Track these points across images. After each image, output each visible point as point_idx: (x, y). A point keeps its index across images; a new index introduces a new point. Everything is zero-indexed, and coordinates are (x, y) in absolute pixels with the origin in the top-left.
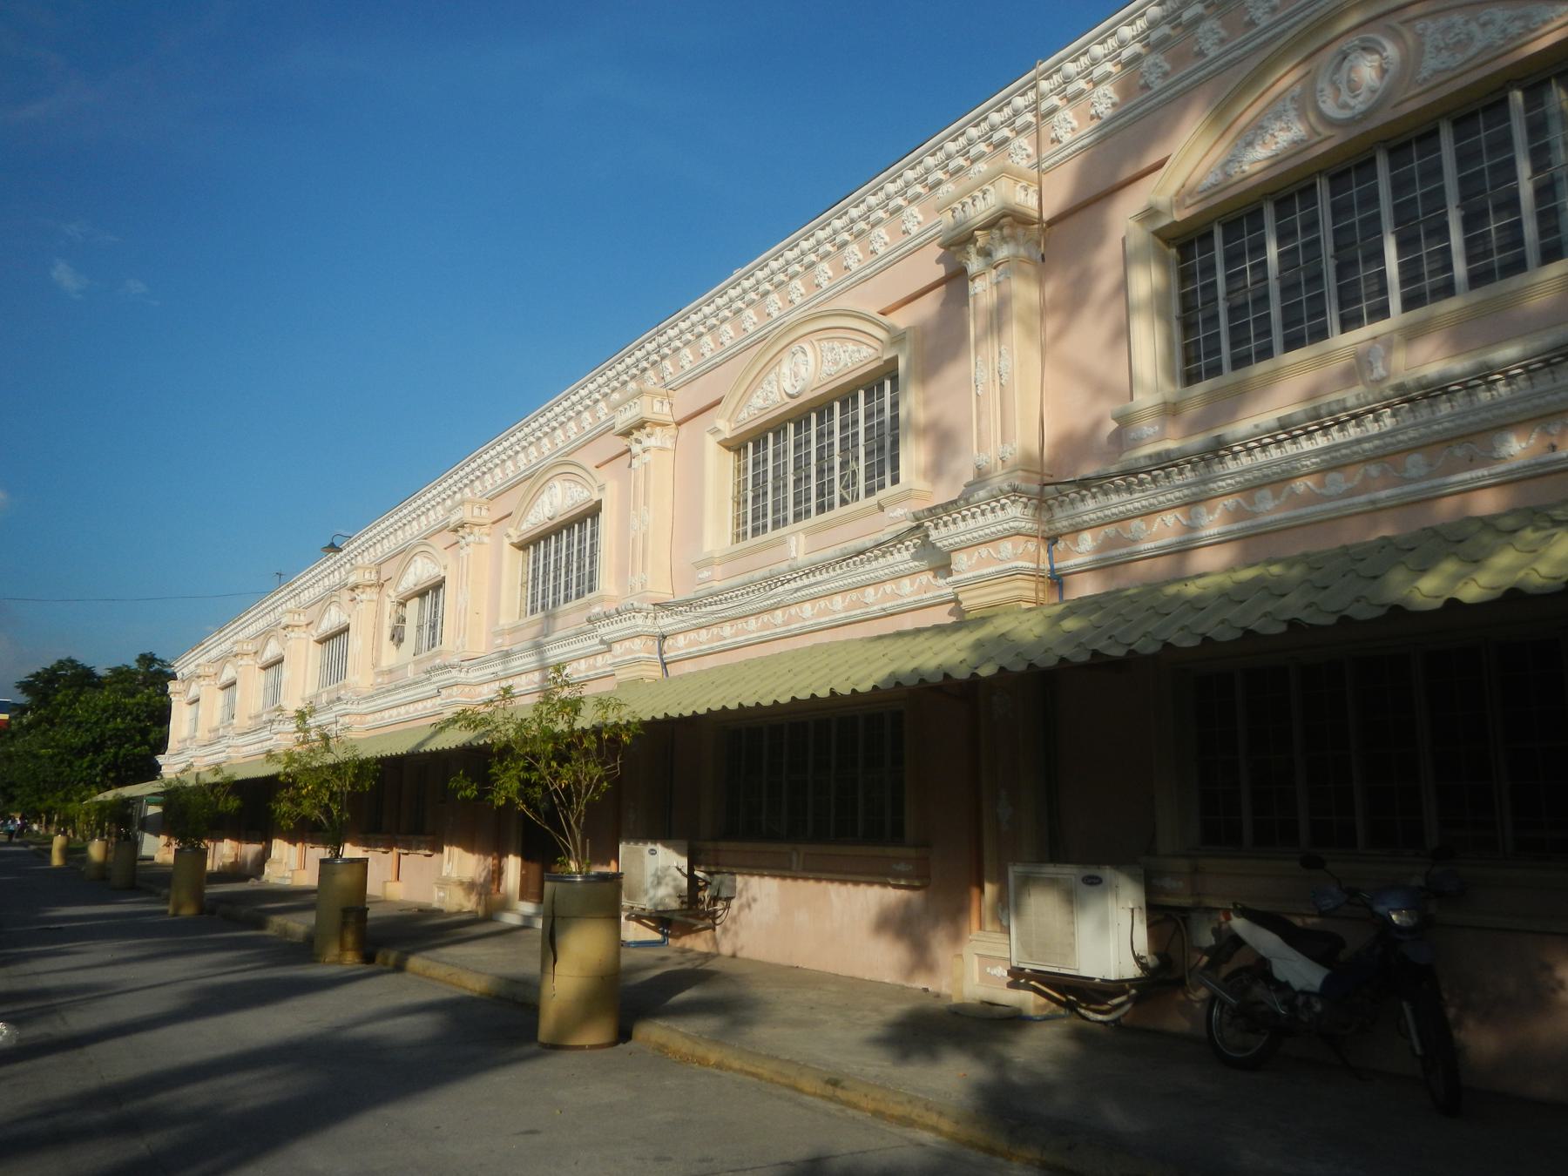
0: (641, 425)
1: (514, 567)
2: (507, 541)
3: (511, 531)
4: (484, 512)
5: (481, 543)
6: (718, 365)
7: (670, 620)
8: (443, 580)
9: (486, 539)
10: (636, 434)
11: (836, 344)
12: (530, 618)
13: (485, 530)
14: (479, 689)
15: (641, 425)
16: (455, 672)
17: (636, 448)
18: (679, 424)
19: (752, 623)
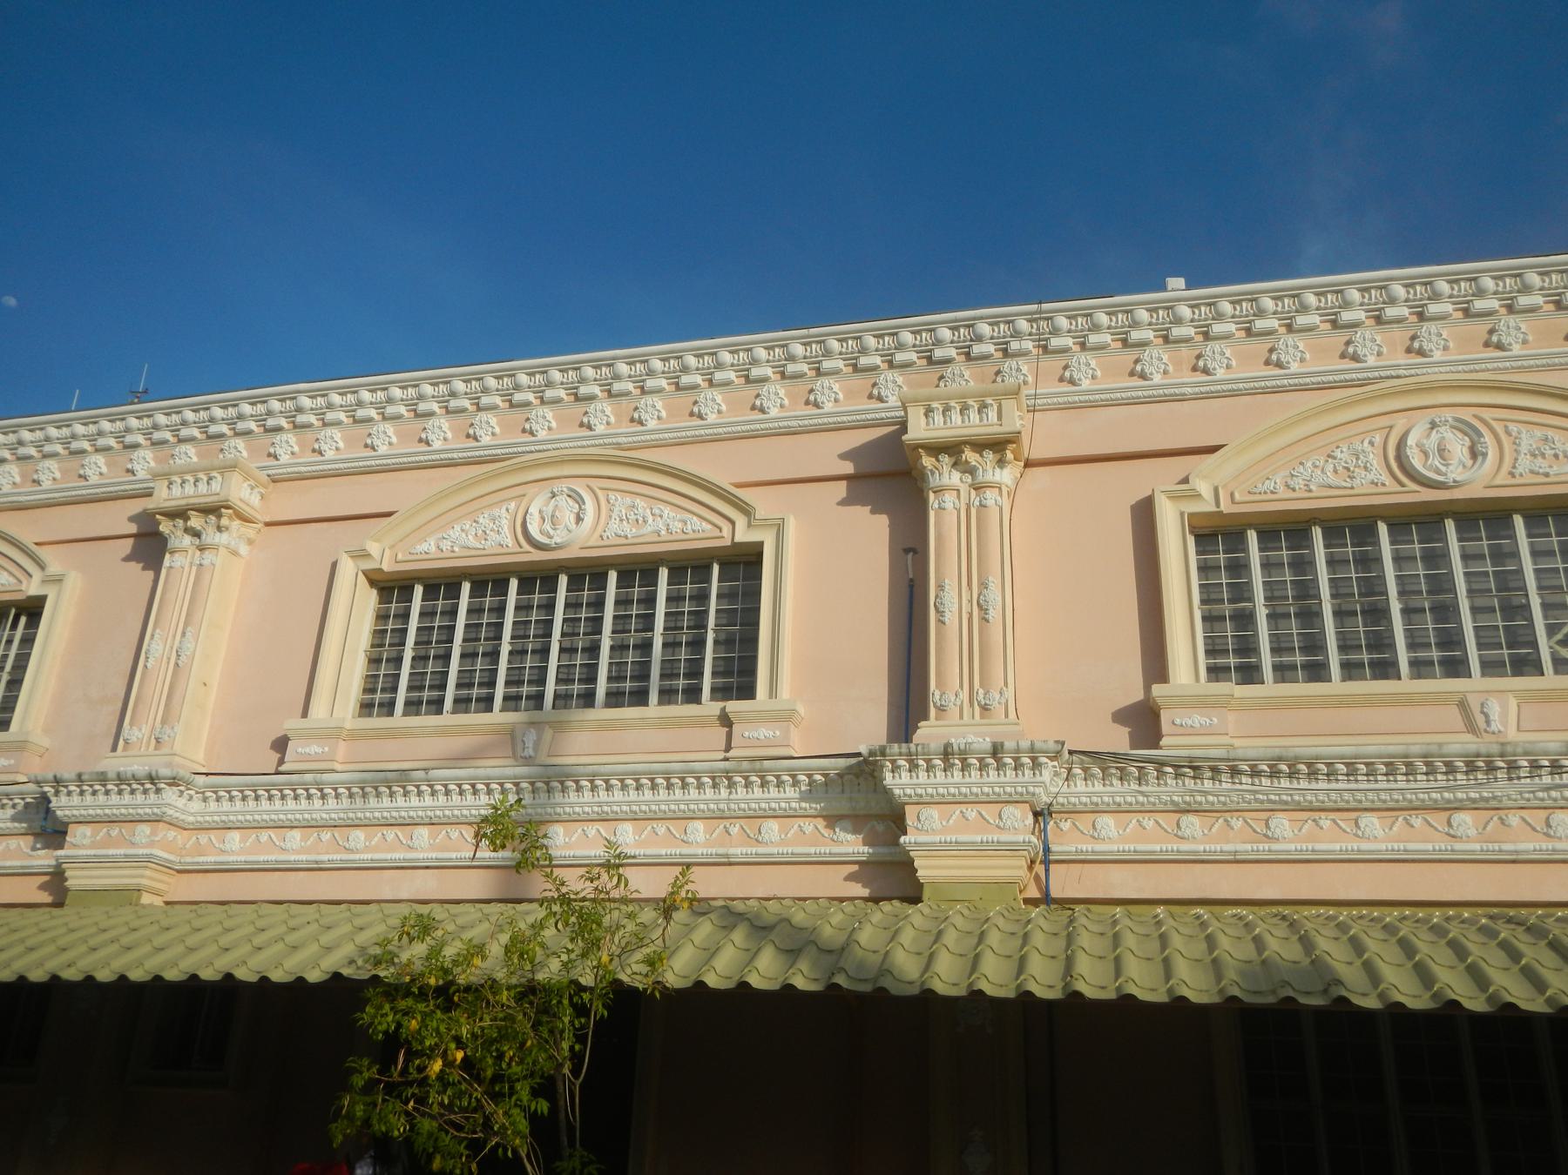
0: (997, 446)
1: (355, 615)
2: (348, 570)
3: (374, 548)
4: (255, 500)
5: (235, 553)
6: (1182, 399)
7: (1098, 787)
8: (32, 610)
9: (244, 549)
10: (970, 456)
11: (1550, 433)
12: (399, 719)
13: (250, 531)
14: (203, 838)
15: (997, 446)
16: (170, 794)
17: (944, 475)
18: (1029, 464)
19: (1371, 822)
